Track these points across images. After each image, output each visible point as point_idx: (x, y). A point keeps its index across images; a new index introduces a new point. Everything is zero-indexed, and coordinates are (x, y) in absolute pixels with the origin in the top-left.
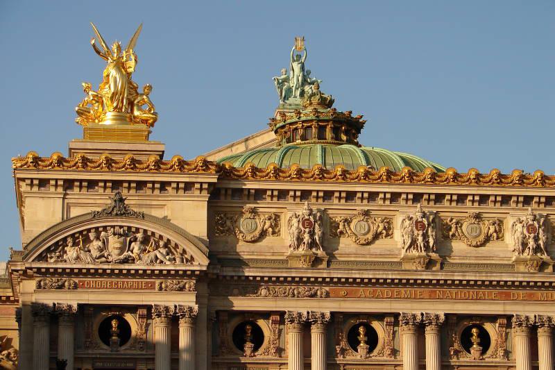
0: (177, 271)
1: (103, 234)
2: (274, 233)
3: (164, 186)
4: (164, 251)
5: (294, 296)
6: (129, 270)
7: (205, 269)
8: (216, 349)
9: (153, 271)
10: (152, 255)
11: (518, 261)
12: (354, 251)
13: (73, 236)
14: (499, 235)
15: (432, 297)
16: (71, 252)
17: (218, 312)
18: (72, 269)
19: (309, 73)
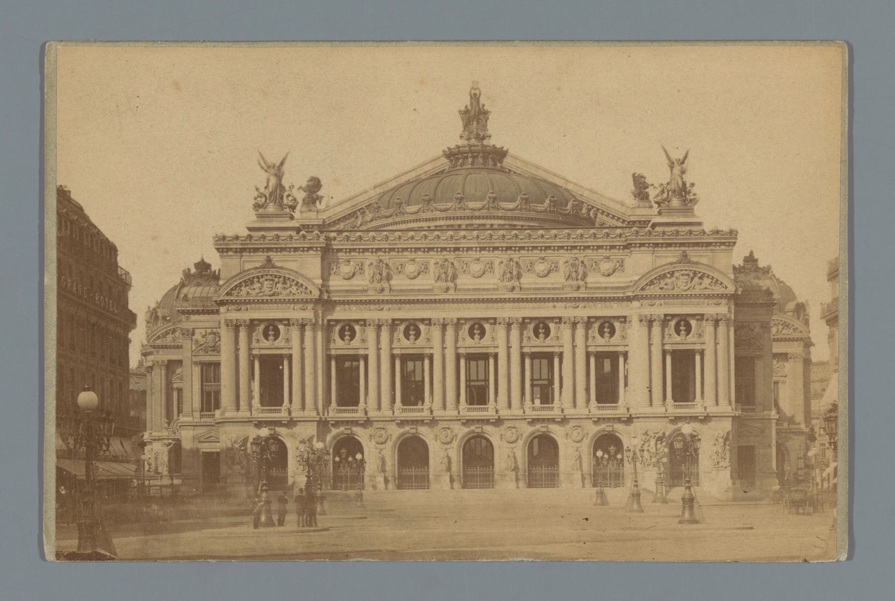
4: (295, 288)
8: (328, 340)
13: (245, 281)
16: (244, 290)
17: (329, 321)
19: (484, 105)
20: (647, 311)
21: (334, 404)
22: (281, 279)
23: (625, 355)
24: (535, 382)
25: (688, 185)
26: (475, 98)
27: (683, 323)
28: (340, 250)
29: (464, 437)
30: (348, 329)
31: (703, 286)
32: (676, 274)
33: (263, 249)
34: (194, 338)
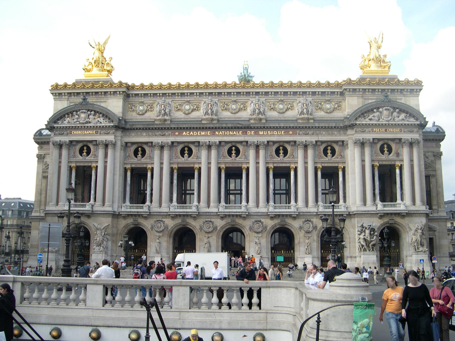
0: (106, 126)
1: (79, 112)
2: (151, 111)
3: (105, 93)
4: (102, 119)
5: (156, 135)
6: (88, 126)
7: (117, 125)
8: (126, 157)
9: (97, 126)
10: (96, 120)
11: (250, 119)
12: (183, 117)
14: (245, 109)
15: (214, 134)
17: (126, 143)
18: (66, 127)
19: (250, 73)
20: (361, 136)
21: (128, 203)
22: (93, 112)
23: (344, 170)
24: (276, 192)
25: (382, 56)
26: (246, 69)
27: (385, 146)
28: (137, 95)
29: (222, 228)
30: (140, 150)
31: (401, 118)
32: (381, 110)
33: (83, 93)
34: (45, 160)
